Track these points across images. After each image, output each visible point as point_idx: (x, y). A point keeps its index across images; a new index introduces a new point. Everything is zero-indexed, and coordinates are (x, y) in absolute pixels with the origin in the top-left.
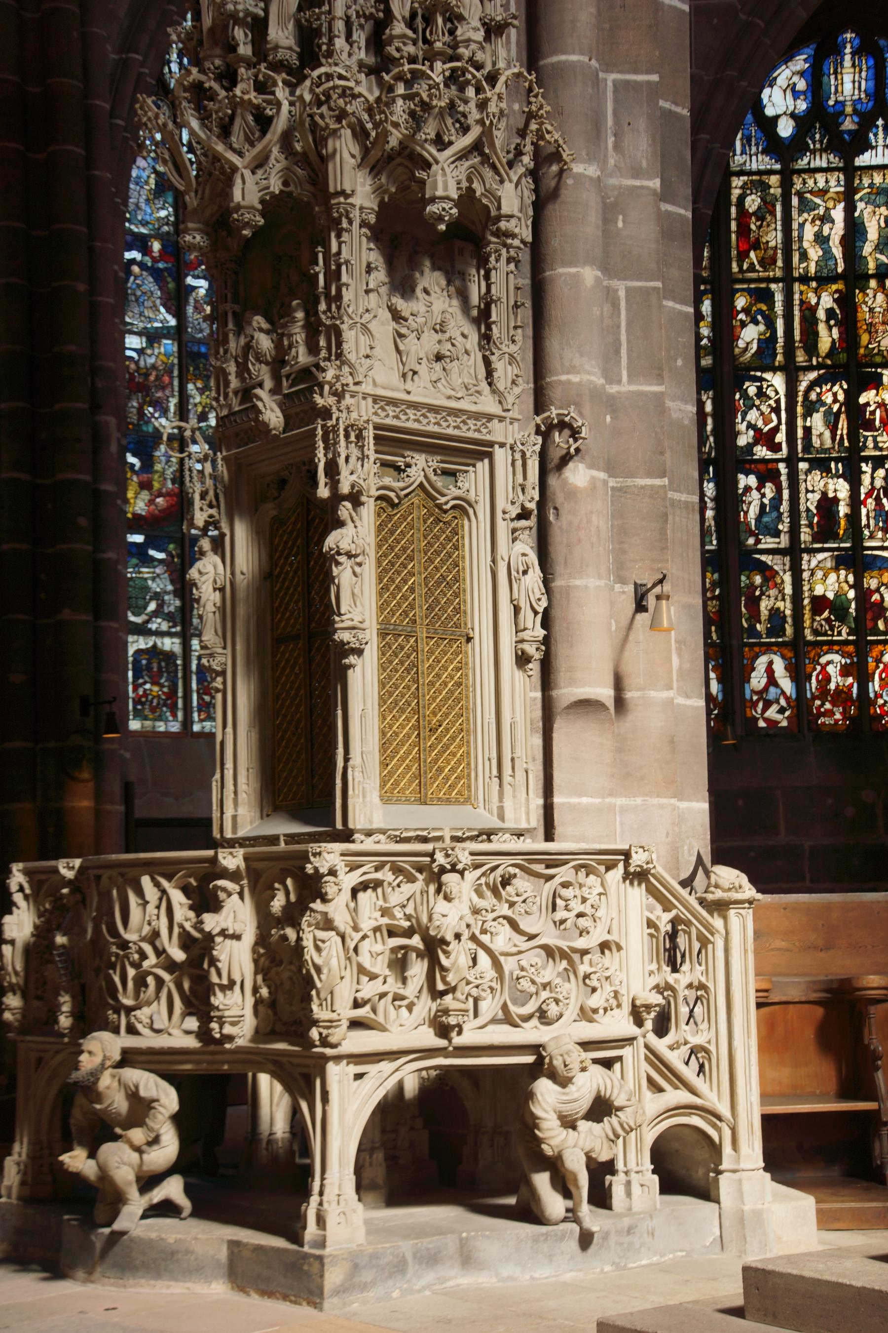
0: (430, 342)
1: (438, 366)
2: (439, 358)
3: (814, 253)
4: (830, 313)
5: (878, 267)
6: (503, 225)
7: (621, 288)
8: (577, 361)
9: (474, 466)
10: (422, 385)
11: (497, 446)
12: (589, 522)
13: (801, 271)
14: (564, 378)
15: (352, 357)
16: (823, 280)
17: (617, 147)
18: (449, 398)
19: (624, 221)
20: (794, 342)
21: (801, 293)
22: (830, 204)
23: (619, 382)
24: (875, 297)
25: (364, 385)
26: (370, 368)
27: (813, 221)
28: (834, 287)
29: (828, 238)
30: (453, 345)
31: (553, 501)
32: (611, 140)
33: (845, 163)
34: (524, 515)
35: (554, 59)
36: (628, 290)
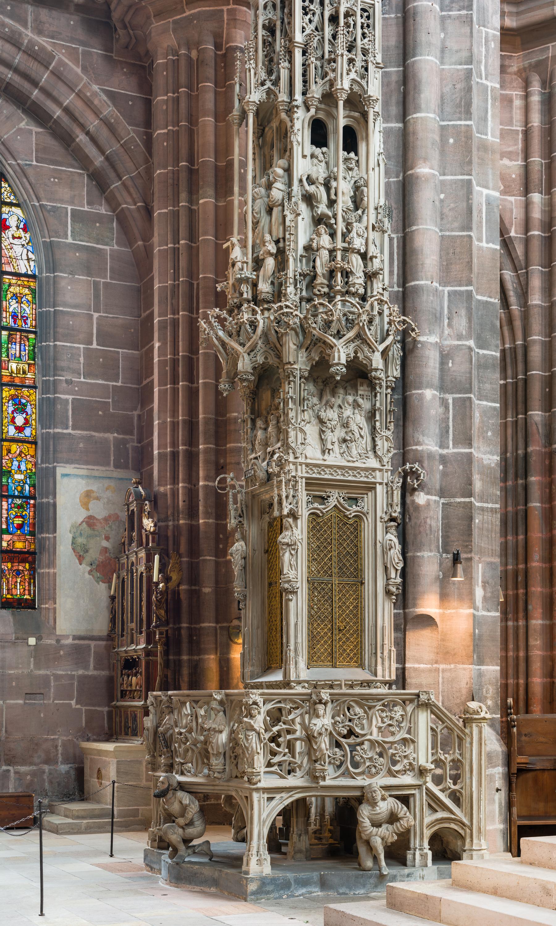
0: (340, 433)
1: (344, 446)
2: (345, 441)
6: (373, 374)
7: (450, 398)
8: (421, 438)
9: (367, 494)
10: (334, 455)
11: (378, 485)
12: (425, 522)
14: (414, 448)
15: (293, 445)
17: (449, 325)
18: (349, 461)
19: (452, 363)
23: (448, 448)
25: (300, 459)
26: (304, 449)
30: (353, 434)
31: (408, 511)
32: (446, 321)
34: (392, 519)
35: (413, 283)
36: (454, 399)
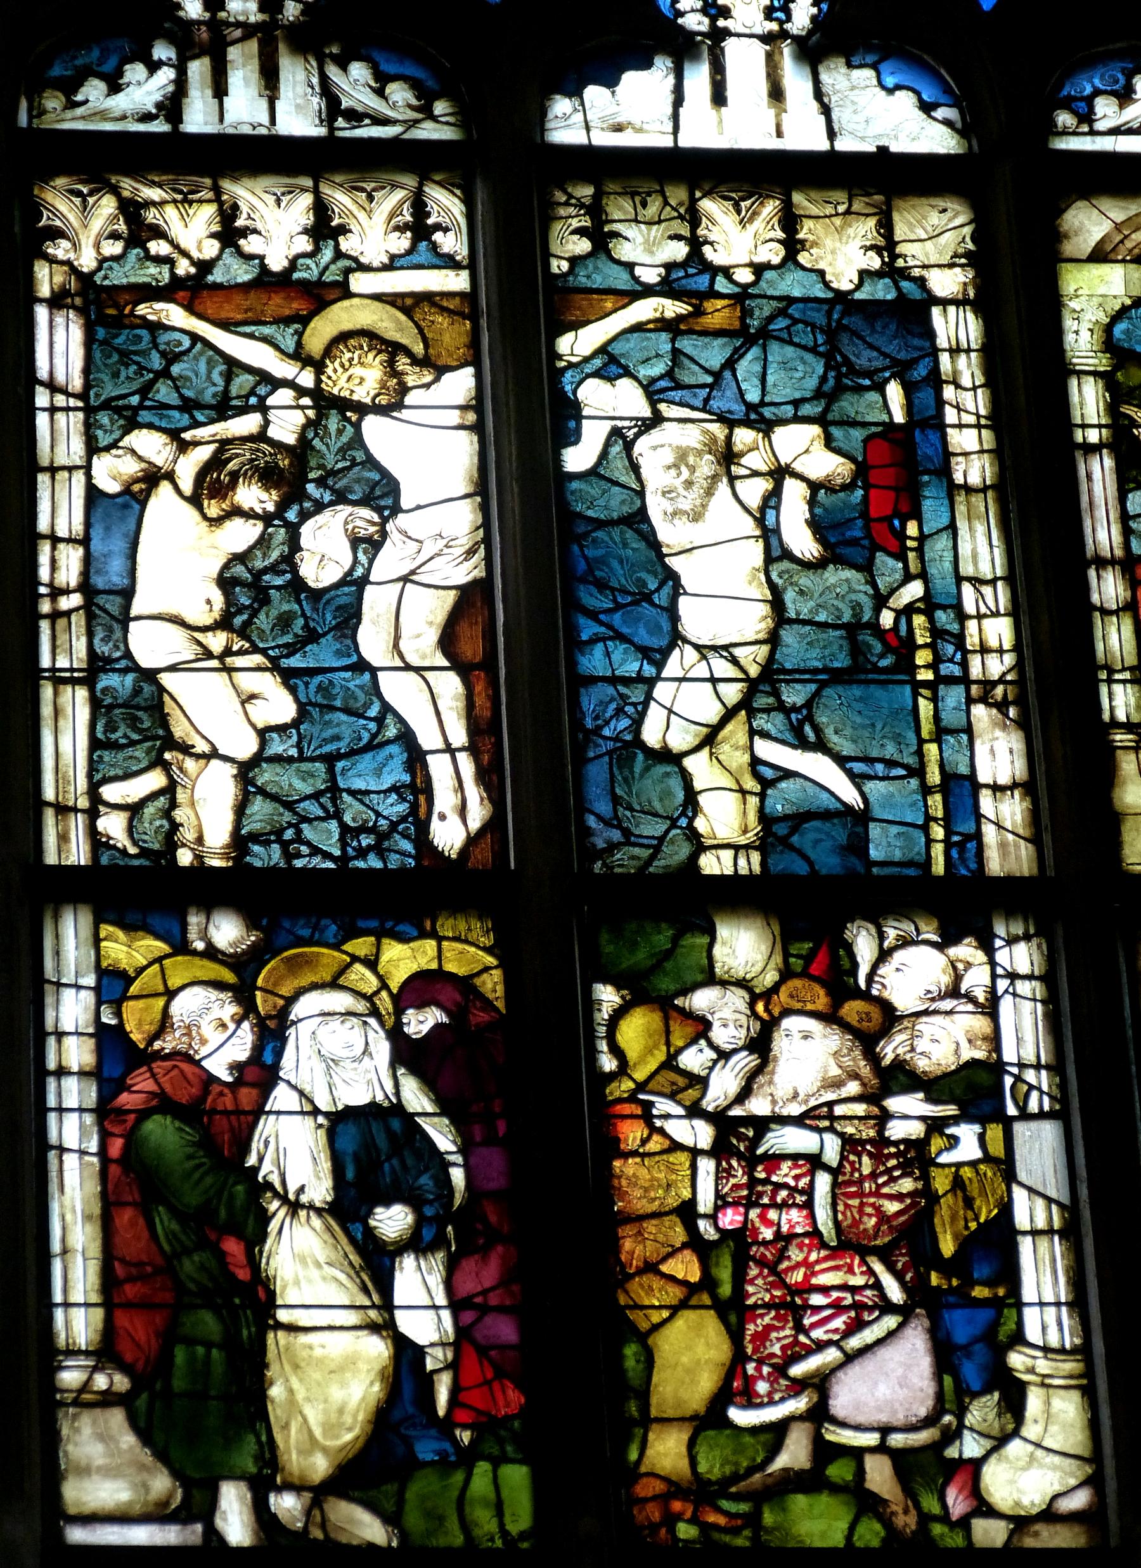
3: (227, 710)
4: (373, 1155)
5: (773, 833)
13: (113, 825)
16: (296, 904)
20: (50, 1355)
21: (113, 985)
22: (361, 378)
24: (760, 1045)
27: (212, 485)
28: (403, 959)
29: (343, 607)
33: (464, 118)
